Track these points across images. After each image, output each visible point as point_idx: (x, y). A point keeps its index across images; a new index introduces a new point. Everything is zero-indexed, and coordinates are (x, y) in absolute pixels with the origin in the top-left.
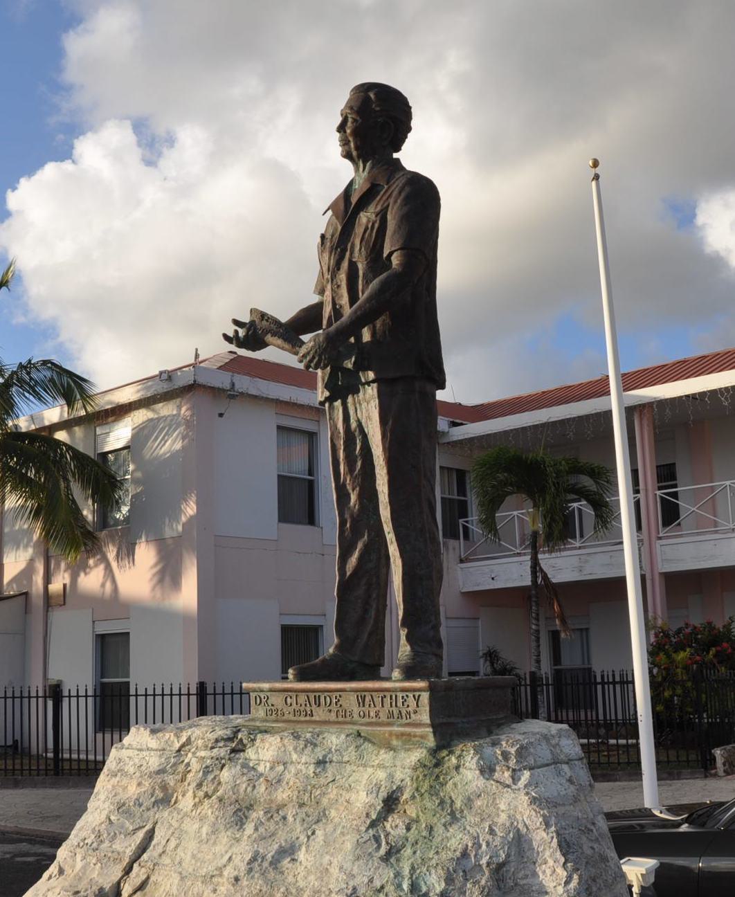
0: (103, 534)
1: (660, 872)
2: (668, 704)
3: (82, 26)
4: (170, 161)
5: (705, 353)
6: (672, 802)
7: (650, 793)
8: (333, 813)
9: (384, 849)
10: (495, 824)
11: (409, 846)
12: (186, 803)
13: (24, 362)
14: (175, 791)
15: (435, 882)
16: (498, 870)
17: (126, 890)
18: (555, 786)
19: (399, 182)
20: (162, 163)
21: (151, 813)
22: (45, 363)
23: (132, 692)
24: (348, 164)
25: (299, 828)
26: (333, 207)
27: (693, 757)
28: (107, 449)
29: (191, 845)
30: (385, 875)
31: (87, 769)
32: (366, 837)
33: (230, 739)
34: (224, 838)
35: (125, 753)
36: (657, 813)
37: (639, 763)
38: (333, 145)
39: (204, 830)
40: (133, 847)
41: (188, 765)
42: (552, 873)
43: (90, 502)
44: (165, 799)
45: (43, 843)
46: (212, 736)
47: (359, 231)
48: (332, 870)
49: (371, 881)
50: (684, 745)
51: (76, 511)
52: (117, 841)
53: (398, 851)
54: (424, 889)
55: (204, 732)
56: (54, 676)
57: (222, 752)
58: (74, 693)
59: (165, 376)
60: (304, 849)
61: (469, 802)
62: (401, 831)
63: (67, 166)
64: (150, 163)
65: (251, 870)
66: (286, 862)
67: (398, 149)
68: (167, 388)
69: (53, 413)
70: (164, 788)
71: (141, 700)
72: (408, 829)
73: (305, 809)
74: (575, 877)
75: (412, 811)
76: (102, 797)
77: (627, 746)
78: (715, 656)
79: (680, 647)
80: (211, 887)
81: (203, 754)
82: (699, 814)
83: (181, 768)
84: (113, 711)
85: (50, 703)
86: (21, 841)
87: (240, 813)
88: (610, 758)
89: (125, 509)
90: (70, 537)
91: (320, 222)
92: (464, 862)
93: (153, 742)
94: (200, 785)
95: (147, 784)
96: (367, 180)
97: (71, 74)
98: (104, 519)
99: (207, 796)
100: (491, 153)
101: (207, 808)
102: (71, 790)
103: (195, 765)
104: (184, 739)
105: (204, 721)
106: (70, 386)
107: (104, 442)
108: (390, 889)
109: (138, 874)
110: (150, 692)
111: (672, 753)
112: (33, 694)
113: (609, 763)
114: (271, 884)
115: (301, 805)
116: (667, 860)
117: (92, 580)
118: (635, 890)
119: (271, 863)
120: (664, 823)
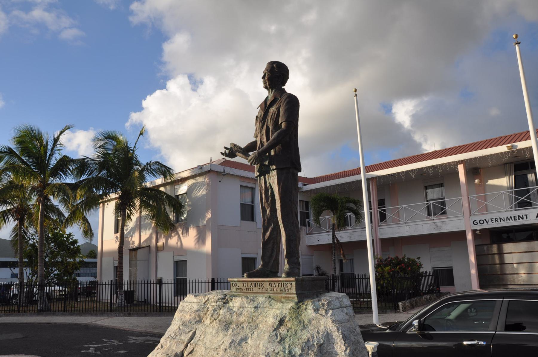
0: (177, 225)
1: (379, 347)
2: (382, 286)
3: (169, 41)
4: (201, 90)
5: (396, 159)
6: (383, 322)
7: (375, 318)
8: (261, 326)
9: (279, 339)
10: (319, 329)
11: (288, 337)
12: (207, 322)
13: (149, 162)
14: (203, 318)
15: (297, 351)
16: (320, 346)
17: (186, 353)
18: (341, 316)
19: (284, 97)
20: (198, 90)
21: (195, 326)
22: (156, 162)
23: (188, 282)
24: (266, 90)
25: (248, 331)
26: (261, 106)
27: (391, 305)
28: (178, 194)
29: (209, 337)
30: (279, 348)
31: (171, 310)
32: (273, 334)
33: (223, 299)
34: (221, 335)
35: (185, 304)
36: (378, 326)
37: (371, 308)
38: (261, 84)
39: (214, 332)
40: (188, 338)
41: (208, 308)
42: (340, 348)
43: (172, 213)
44: (200, 321)
45: (155, 337)
46: (217, 298)
47: (270, 115)
48: (260, 346)
49: (274, 350)
50: (388, 301)
51: (167, 216)
52: (182, 336)
53: (284, 339)
54: (294, 353)
55: (214, 296)
56: (159, 276)
57: (220, 303)
58: (166, 282)
59: (200, 167)
60: (250, 338)
61: (310, 322)
62: (285, 332)
63: (164, 91)
64: (194, 90)
65: (231, 346)
66: (243, 343)
67: (284, 85)
68: (201, 172)
69: (159, 181)
70: (199, 316)
71: (191, 284)
72: (288, 331)
73: (250, 324)
74: (348, 349)
75: (289, 325)
76: (177, 320)
77: (367, 301)
78: (399, 269)
79: (386, 265)
80: (216, 352)
81: (213, 304)
82: (393, 326)
83: (205, 309)
84: (181, 289)
85: (158, 286)
86: (147, 336)
87: (226, 325)
88: (361, 306)
89: (185, 216)
90: (165, 225)
91: (256, 111)
92: (308, 343)
93: (195, 300)
94: (212, 316)
95: (193, 315)
96: (273, 96)
97: (166, 57)
98: (177, 219)
99: (215, 319)
100: (318, 86)
101: (215, 324)
102: (166, 317)
103: (211, 308)
104: (206, 299)
105: (214, 292)
106: (165, 171)
107: (178, 191)
108: (281, 353)
109: (190, 348)
110: (194, 282)
111: (384, 304)
112: (152, 282)
113: (361, 308)
114: (238, 351)
115: (249, 323)
116: (381, 343)
117: (173, 241)
118: (370, 353)
119: (238, 344)
120: (381, 329)
